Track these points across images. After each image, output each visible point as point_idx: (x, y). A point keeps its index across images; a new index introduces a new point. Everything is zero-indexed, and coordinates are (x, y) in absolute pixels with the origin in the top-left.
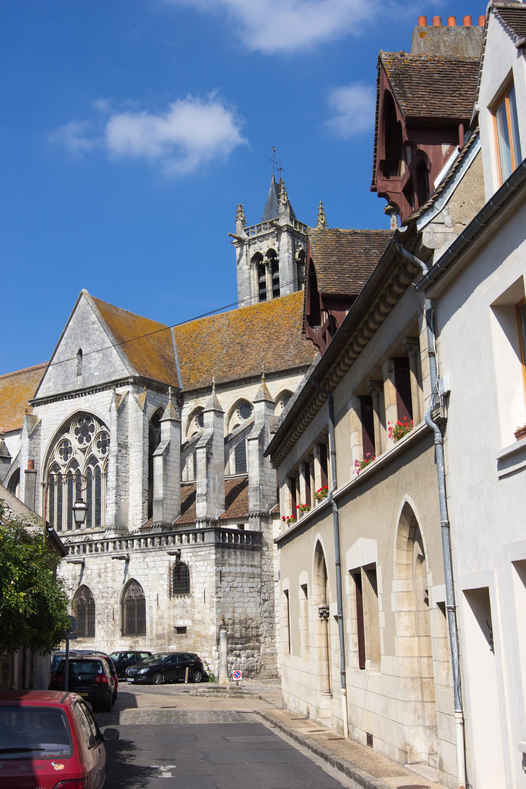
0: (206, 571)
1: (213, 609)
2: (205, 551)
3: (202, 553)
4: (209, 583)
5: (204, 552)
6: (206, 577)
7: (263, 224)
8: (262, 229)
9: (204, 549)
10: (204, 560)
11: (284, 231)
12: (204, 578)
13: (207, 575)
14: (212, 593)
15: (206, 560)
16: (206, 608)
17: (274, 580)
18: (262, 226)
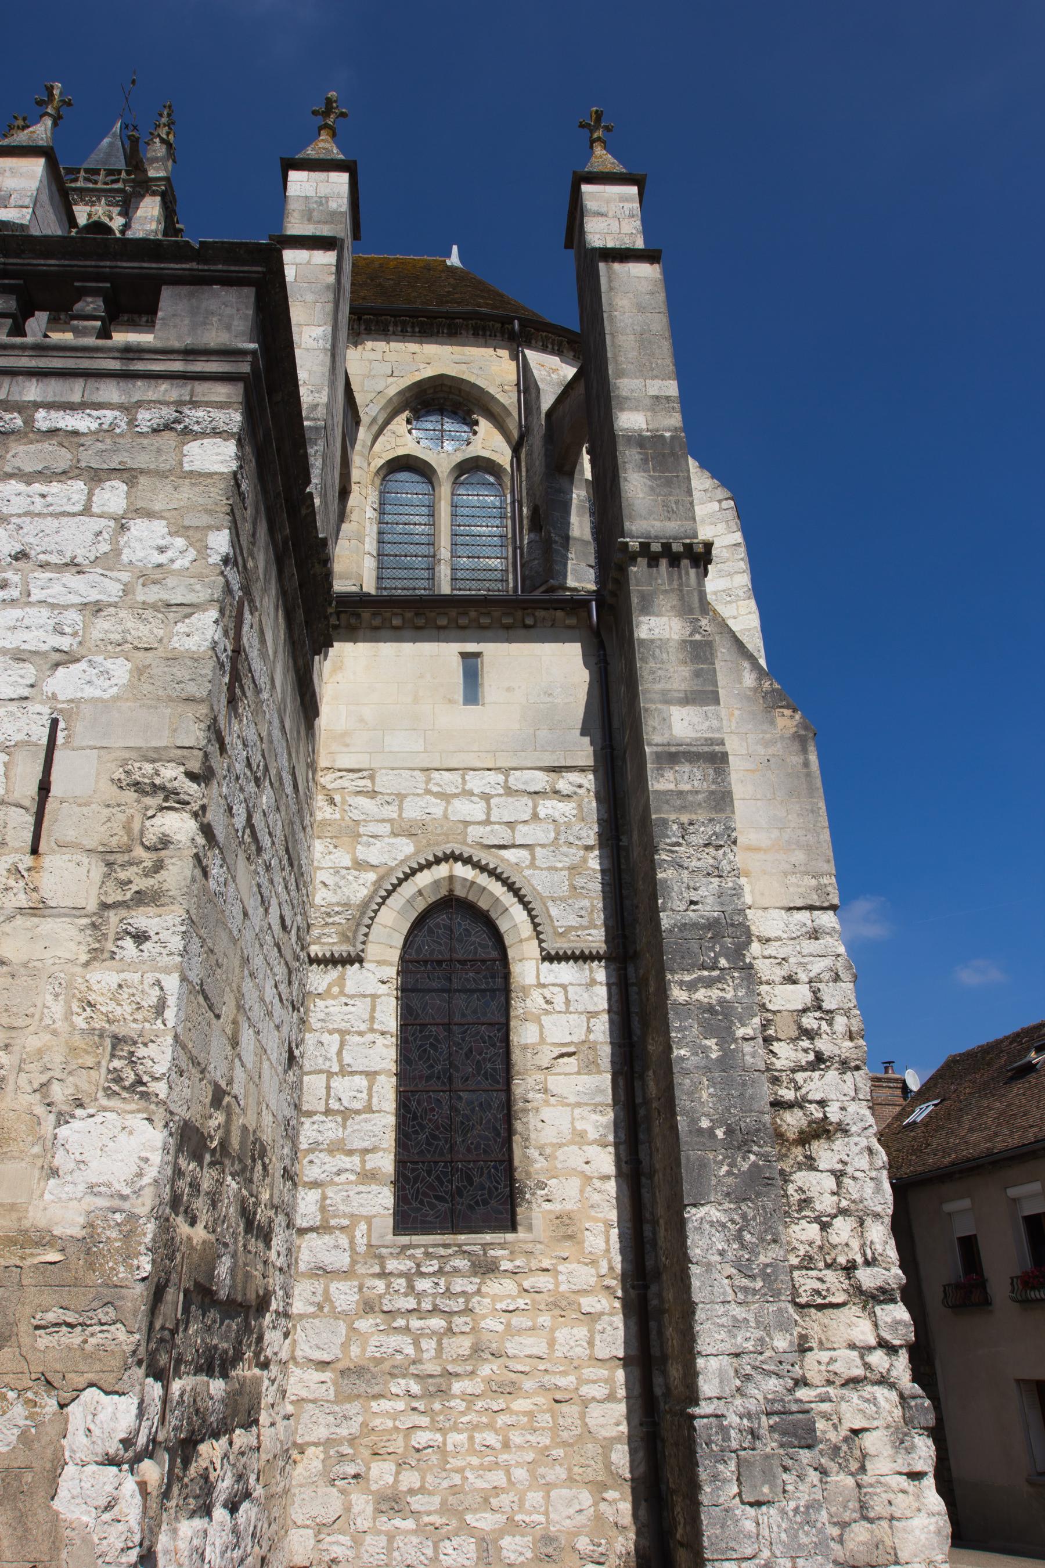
0: (109, 561)
1: (142, 919)
2: (129, 409)
3: (80, 422)
4: (121, 670)
5: (109, 415)
6: (97, 609)
7: (87, 171)
8: (81, 179)
9: (110, 392)
10: (96, 477)
11: (154, 194)
12: (73, 616)
13: (111, 590)
14: (154, 756)
15: (129, 475)
16: (39, 909)
17: (315, 950)
18: (82, 173)
